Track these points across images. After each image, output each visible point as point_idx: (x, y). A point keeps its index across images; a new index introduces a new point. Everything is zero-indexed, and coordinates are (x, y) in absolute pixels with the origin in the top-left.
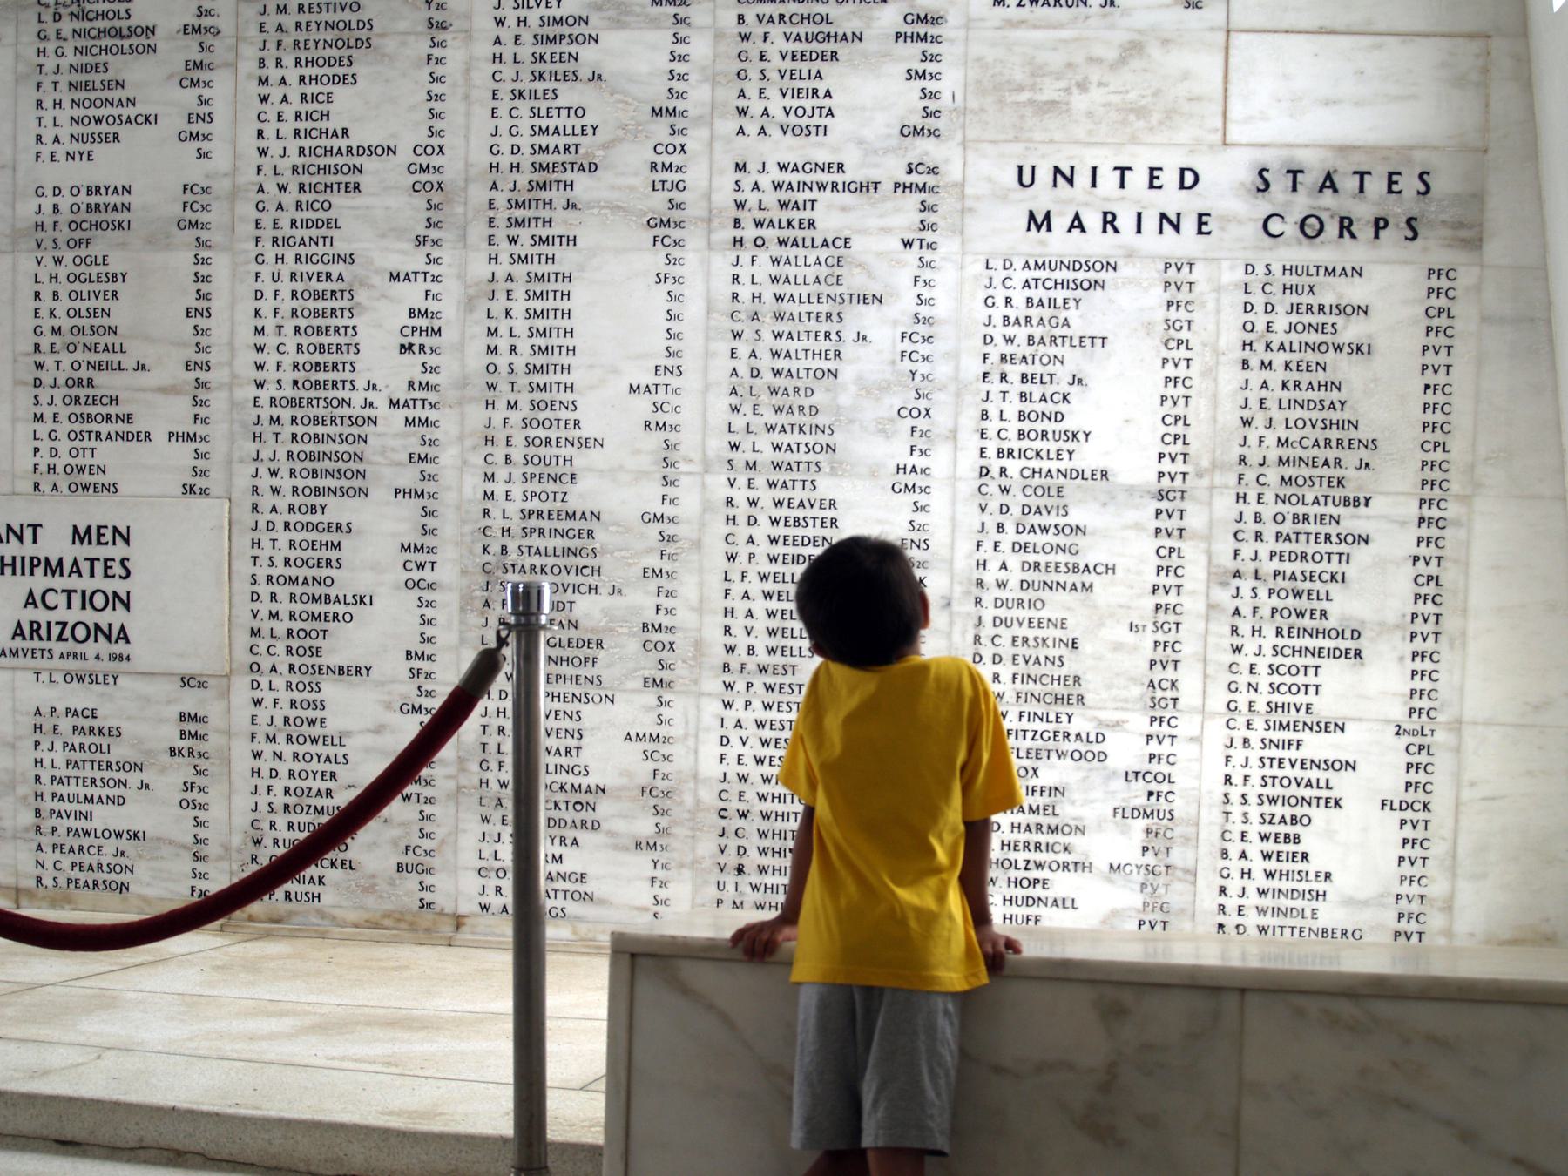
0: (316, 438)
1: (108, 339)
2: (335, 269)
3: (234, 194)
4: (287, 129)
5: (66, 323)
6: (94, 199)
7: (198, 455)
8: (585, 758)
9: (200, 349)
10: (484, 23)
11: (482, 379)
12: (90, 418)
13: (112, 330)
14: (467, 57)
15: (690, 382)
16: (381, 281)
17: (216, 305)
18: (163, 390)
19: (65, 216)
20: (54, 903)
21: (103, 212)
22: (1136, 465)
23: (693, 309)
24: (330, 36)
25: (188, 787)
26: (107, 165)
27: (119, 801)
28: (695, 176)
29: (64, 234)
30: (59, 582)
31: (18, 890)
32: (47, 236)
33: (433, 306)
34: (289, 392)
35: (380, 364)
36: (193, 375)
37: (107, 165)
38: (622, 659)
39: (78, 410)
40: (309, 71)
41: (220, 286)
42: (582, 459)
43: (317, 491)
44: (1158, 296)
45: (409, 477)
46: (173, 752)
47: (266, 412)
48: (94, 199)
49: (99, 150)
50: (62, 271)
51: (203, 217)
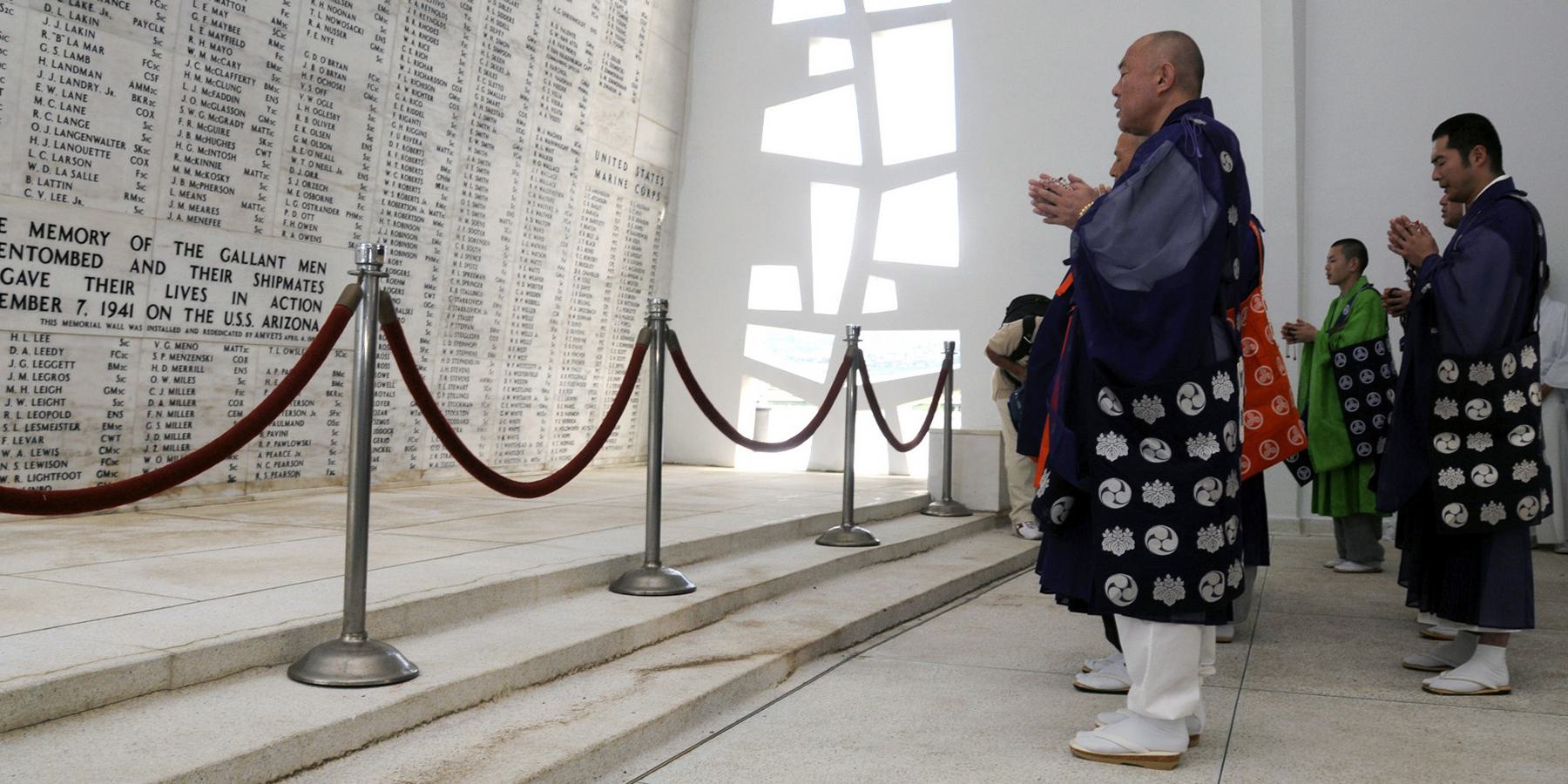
0: (402, 225)
1: (326, 152)
2: (420, 138)
3: (388, 86)
4: (413, 58)
5: (310, 138)
6: (331, 68)
7: (358, 227)
8: (468, 391)
9: (366, 168)
10: (480, 33)
11: (459, 206)
12: (313, 197)
13: (329, 147)
14: (475, 45)
15: (515, 220)
16: (434, 148)
17: (375, 144)
18: (347, 187)
19: (316, 74)
20: (264, 488)
21: (330, 78)
22: (604, 275)
23: (520, 188)
24: (433, 16)
25: (333, 413)
26: (339, 50)
27: (300, 424)
28: (527, 128)
29: (315, 84)
30: (290, 293)
31: (246, 483)
32: (307, 82)
33: (449, 167)
34: (395, 199)
35: (429, 194)
36: (360, 181)
37: (339, 50)
38: (483, 345)
39: (309, 190)
40: (424, 32)
41: (377, 135)
42: (485, 250)
43: (400, 253)
44: (615, 209)
45: (431, 253)
46: (329, 393)
47: (387, 208)
48: (331, 68)
49: (336, 38)
50: (312, 105)
51: (375, 95)
